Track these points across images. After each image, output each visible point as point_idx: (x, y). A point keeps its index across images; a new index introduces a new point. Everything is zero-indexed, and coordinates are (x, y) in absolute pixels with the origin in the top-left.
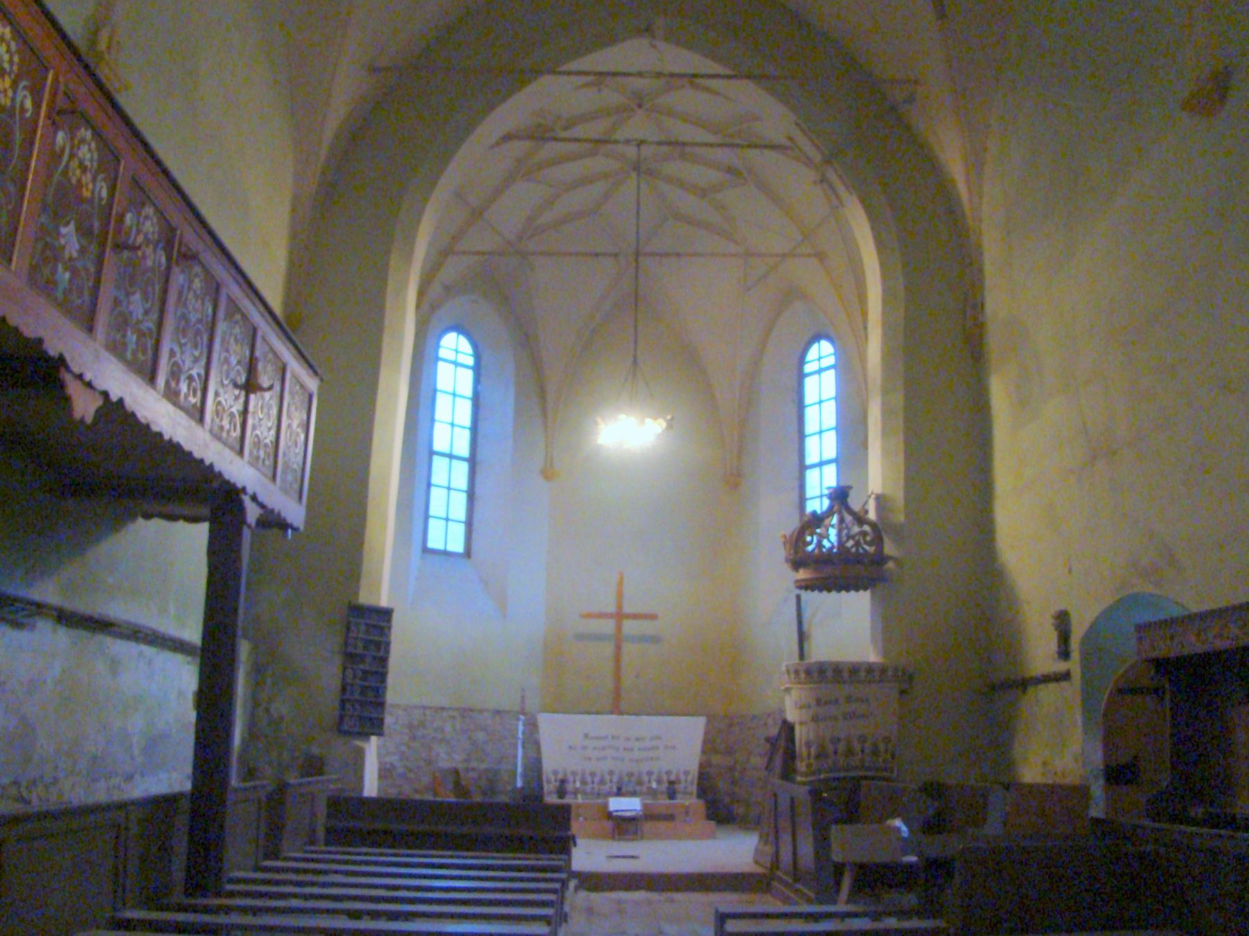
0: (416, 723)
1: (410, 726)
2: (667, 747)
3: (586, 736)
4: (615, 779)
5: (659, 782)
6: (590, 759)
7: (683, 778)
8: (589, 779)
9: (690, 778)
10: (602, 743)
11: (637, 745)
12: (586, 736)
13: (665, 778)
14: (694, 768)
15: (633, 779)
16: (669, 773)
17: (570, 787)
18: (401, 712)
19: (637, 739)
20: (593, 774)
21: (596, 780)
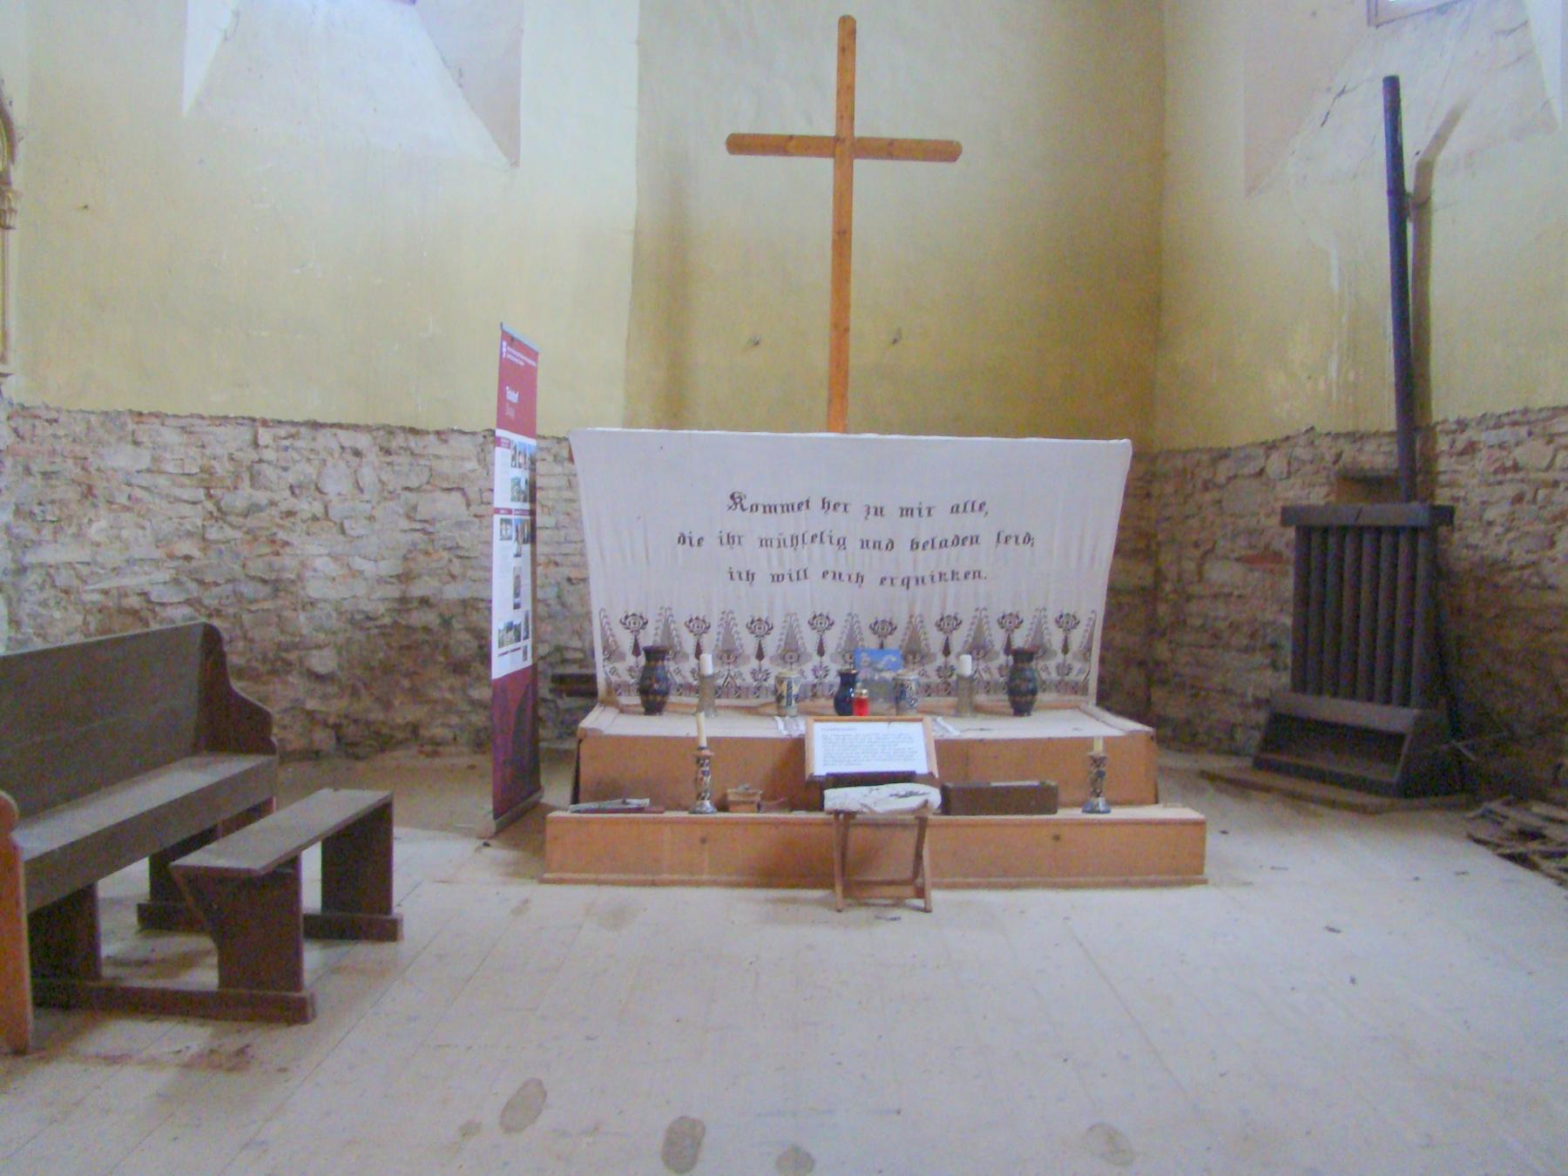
0: (222, 468)
1: (207, 481)
2: (1002, 539)
3: (736, 499)
4: (833, 639)
5: (978, 649)
6: (750, 576)
7: (1055, 638)
8: (748, 643)
9: (1077, 638)
10: (788, 524)
11: (907, 529)
12: (736, 499)
13: (997, 638)
14: (1089, 601)
15: (893, 642)
16: (1010, 622)
17: (679, 670)
18: (170, 436)
19: (906, 512)
20: (759, 627)
21: (772, 644)
